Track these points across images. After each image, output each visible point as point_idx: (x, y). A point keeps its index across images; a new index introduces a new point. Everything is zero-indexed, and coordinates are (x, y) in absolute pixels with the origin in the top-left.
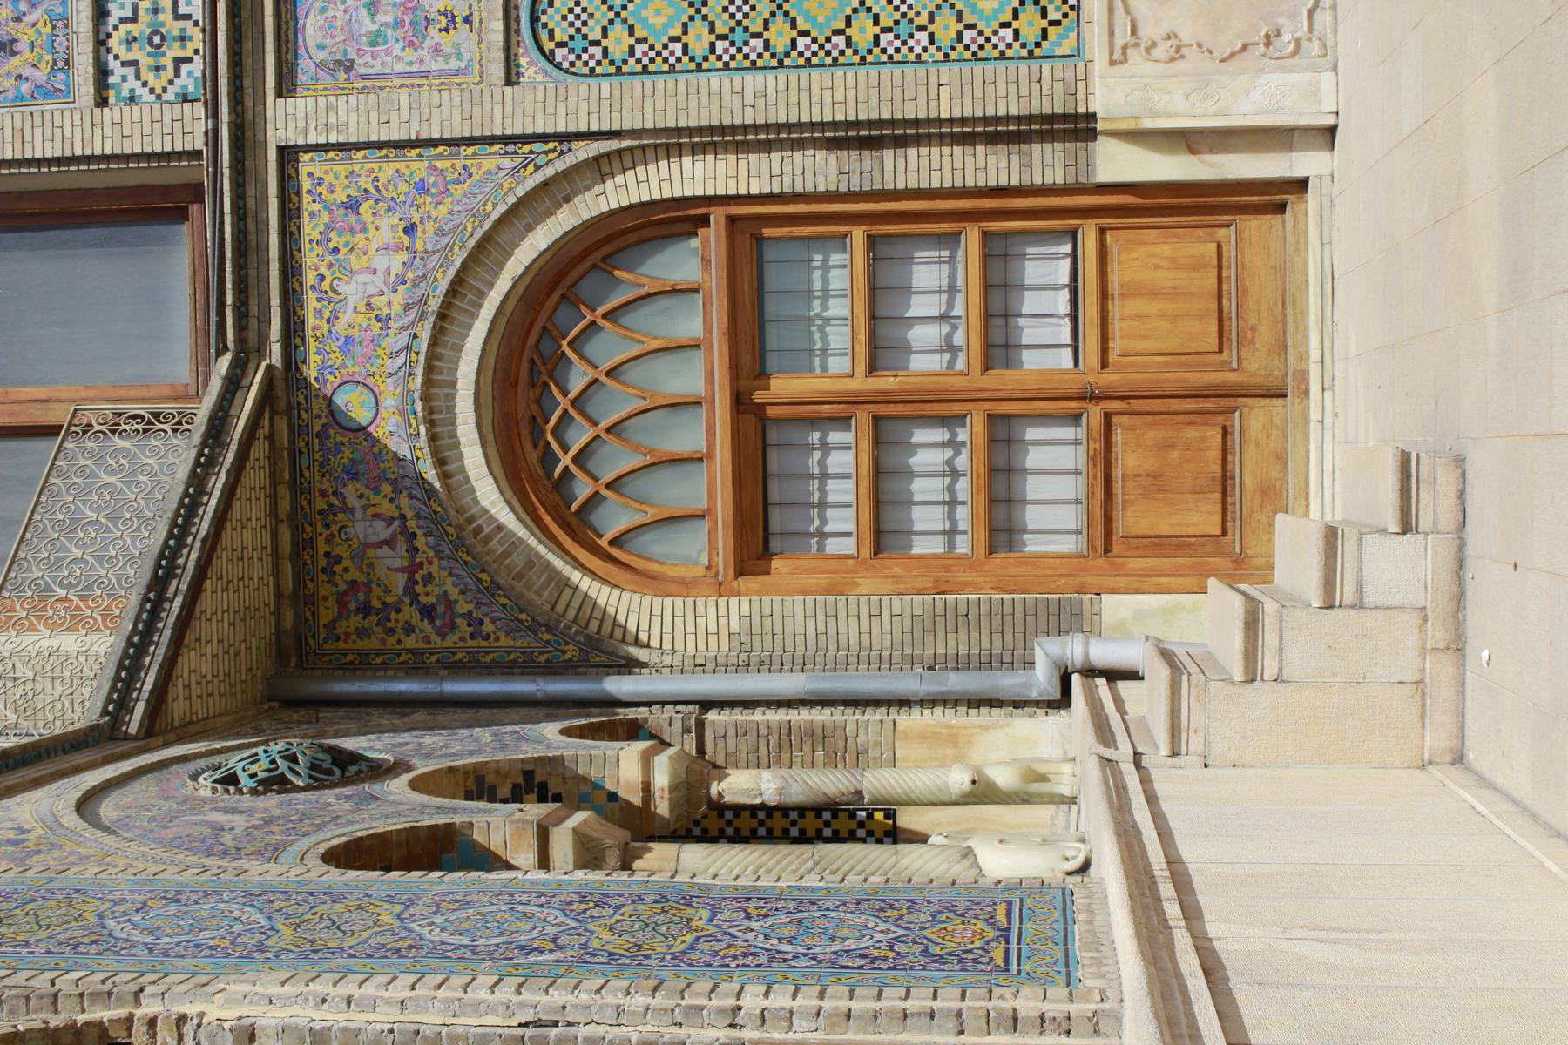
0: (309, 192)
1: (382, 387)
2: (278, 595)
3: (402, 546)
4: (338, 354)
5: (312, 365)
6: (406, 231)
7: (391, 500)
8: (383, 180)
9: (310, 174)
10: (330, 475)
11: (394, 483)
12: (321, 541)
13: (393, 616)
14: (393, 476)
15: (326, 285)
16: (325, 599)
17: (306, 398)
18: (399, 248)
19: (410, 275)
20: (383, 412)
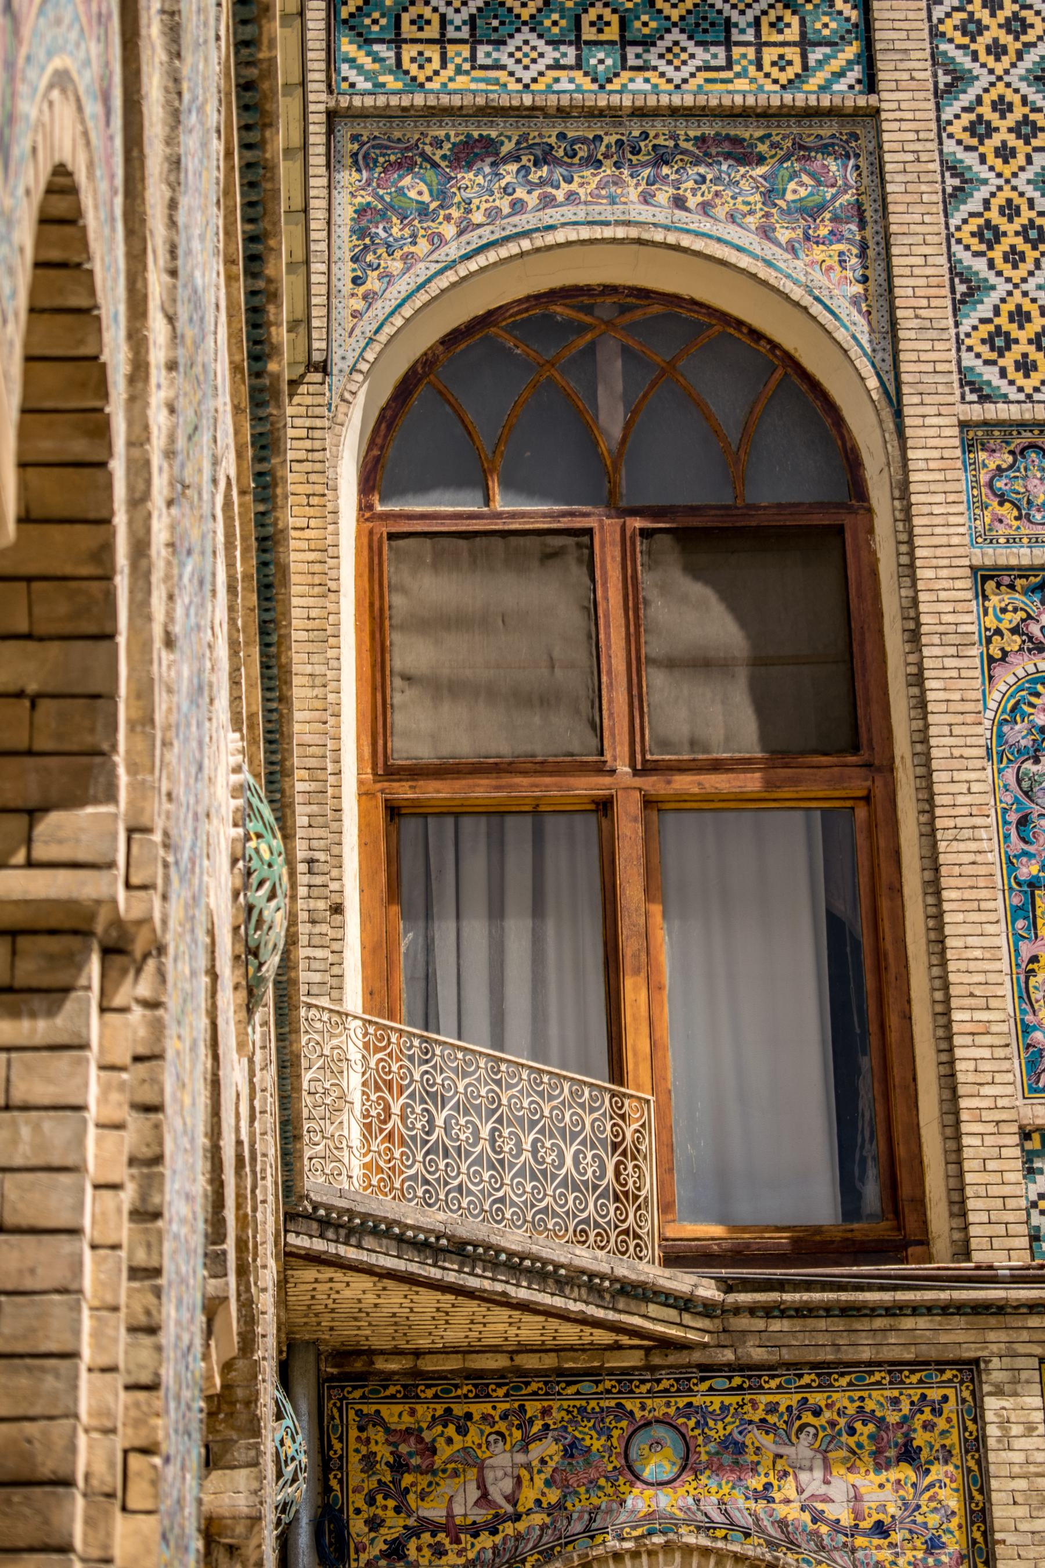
0: (924, 1397)
1: (681, 1491)
2: (417, 1354)
3: (481, 1515)
4: (721, 1433)
5: (708, 1399)
6: (879, 1524)
7: (538, 1502)
8: (942, 1494)
9: (945, 1399)
10: (570, 1421)
11: (560, 1506)
12: (487, 1408)
13: (391, 1503)
14: (569, 1505)
15: (808, 1417)
16: (413, 1413)
17: (666, 1390)
18: (858, 1515)
19: (824, 1529)
20: (650, 1492)
